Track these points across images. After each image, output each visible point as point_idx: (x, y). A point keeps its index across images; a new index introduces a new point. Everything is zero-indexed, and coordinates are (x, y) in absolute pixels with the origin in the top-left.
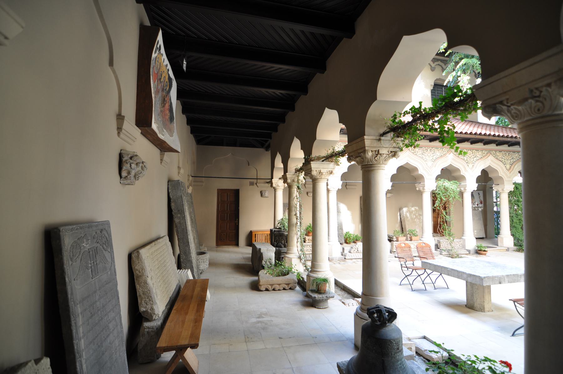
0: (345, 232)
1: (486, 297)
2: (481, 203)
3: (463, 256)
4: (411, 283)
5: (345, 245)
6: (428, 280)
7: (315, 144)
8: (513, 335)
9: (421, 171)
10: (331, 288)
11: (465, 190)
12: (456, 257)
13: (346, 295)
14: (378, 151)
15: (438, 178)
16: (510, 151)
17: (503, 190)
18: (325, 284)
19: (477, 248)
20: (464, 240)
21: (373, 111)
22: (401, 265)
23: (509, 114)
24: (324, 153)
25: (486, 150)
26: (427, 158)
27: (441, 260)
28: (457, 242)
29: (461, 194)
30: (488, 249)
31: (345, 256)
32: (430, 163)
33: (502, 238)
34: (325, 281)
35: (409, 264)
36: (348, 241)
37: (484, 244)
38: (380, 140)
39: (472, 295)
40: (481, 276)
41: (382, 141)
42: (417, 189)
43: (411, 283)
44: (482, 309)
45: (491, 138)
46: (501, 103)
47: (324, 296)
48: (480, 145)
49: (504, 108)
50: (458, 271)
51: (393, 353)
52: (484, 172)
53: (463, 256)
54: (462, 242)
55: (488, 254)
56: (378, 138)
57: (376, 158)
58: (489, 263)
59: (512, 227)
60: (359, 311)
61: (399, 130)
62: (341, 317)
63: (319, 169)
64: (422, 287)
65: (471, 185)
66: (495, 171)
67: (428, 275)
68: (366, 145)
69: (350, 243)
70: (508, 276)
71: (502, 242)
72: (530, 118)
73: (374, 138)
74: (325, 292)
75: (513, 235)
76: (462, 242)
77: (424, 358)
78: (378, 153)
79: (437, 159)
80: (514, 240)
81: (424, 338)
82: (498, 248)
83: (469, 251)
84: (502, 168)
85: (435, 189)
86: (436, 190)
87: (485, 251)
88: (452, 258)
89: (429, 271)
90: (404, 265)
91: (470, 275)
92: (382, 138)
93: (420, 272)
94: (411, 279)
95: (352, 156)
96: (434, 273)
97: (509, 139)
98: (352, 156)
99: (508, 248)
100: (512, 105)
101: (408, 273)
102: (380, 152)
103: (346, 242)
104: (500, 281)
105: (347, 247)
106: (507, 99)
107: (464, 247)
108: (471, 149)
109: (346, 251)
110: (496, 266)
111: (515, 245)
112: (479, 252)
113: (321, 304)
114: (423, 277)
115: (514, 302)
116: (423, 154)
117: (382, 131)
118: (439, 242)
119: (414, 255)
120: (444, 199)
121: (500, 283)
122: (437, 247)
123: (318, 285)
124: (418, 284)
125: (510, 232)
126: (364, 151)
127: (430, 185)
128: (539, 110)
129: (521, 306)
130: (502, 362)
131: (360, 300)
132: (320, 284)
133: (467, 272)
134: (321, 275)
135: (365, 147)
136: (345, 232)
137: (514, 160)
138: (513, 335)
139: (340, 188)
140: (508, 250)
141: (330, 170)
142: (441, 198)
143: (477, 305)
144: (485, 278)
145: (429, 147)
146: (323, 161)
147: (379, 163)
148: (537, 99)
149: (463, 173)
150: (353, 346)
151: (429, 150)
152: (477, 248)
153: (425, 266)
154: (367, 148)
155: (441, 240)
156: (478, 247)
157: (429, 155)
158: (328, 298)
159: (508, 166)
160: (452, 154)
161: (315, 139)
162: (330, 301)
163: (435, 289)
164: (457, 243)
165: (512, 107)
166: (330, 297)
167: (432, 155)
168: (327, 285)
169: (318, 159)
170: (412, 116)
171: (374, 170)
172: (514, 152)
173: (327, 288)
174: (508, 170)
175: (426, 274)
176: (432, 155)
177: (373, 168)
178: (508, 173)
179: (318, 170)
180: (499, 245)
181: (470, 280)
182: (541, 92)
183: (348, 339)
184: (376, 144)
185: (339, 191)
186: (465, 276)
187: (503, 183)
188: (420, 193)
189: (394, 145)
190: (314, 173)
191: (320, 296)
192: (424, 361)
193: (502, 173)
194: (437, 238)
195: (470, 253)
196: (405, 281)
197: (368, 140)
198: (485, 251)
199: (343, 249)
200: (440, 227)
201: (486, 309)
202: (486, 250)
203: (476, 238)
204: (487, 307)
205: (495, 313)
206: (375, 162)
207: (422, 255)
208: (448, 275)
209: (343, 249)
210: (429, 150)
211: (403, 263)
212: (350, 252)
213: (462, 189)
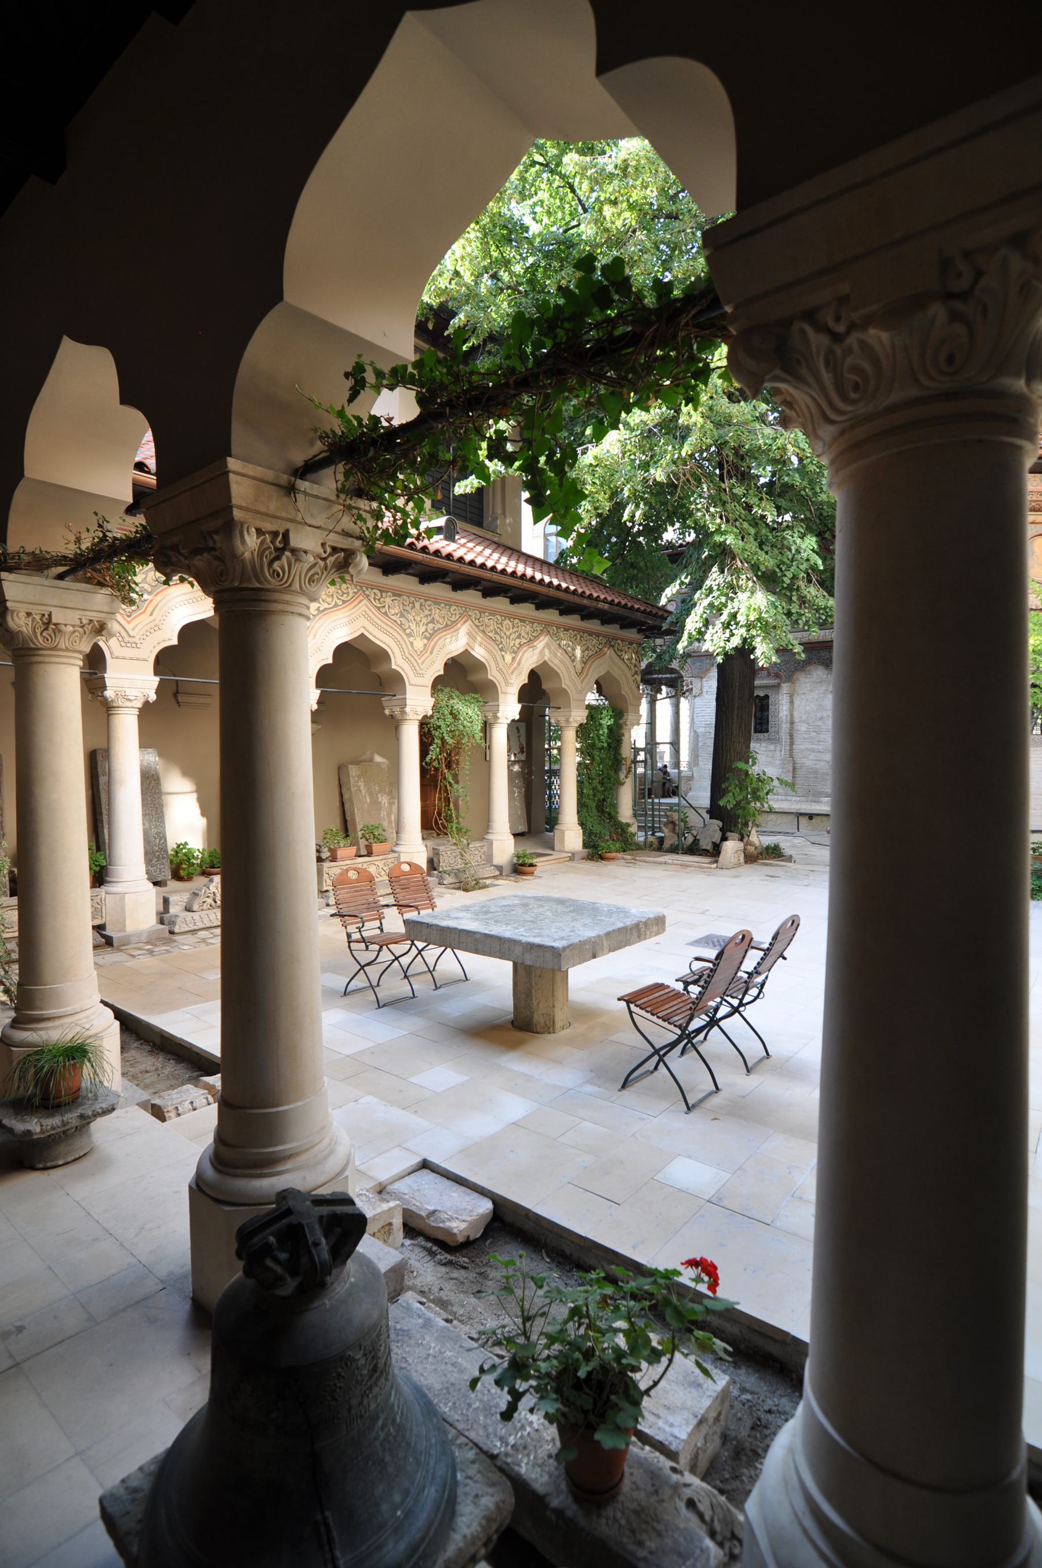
0: (171, 845)
1: (559, 994)
2: (522, 752)
3: (488, 882)
4: (375, 983)
5: (173, 884)
6: (419, 966)
7: (20, 496)
8: (623, 1087)
9: (398, 663)
10: (110, 1061)
11: (496, 717)
12: (474, 889)
13: (170, 1067)
14: (286, 535)
15: (438, 684)
16: (584, 632)
17: (567, 721)
18: (77, 1069)
19: (515, 860)
20: (490, 843)
21: (266, 351)
22: (349, 936)
23: (826, 377)
24: (62, 542)
25: (539, 622)
26: (413, 627)
27: (450, 907)
28: (477, 849)
29: (486, 727)
30: (538, 860)
31: (172, 923)
32: (419, 643)
33: (563, 832)
34: (77, 1053)
35: (371, 929)
36: (182, 873)
37: (529, 847)
38: (290, 490)
39: (529, 995)
40: (556, 944)
41: (300, 497)
42: (387, 712)
43: (375, 983)
44: (549, 1028)
45: (552, 592)
46: (810, 315)
47: (71, 1117)
48: (526, 609)
49: (817, 340)
50: (499, 939)
51: (354, 1402)
52: (533, 675)
53: (488, 882)
54: (485, 849)
55: (538, 871)
56: (284, 479)
57: (276, 565)
58: (561, 902)
59: (581, 805)
60: (210, 1172)
61: (368, 458)
62: (146, 1165)
63: (45, 610)
64: (403, 988)
65: (510, 709)
66: (555, 675)
67: (420, 952)
68: (235, 501)
69: (189, 878)
70: (608, 934)
71: (562, 841)
72: (913, 392)
73: (270, 475)
74: (75, 1098)
75: (582, 824)
76: (485, 849)
77: (428, 1238)
78: (282, 545)
79: (435, 631)
80: (584, 834)
81: (425, 1165)
82: (556, 855)
83: (500, 868)
84: (567, 668)
85: (430, 713)
86: (432, 716)
87: (531, 865)
88: (466, 890)
89: (420, 945)
90: (356, 936)
91: (531, 947)
92: (303, 485)
93: (399, 949)
94: (373, 972)
95: (175, 548)
96: (431, 946)
97: (585, 602)
98: (175, 548)
99: (573, 854)
100: (852, 327)
101: (365, 957)
102: (295, 541)
103: (177, 876)
104: (590, 950)
105: (179, 894)
106: (843, 300)
107: (489, 858)
108: (511, 617)
109: (173, 910)
110: (577, 908)
111: (585, 845)
112: (520, 868)
113: (62, 1148)
114: (405, 961)
115: (628, 1002)
116: (402, 616)
117: (299, 457)
118: (436, 852)
119: (383, 901)
120: (450, 741)
121: (594, 957)
122: (432, 864)
123: (44, 1081)
124: (394, 986)
125: (576, 817)
126: (229, 527)
127: (418, 702)
128: (951, 359)
129: (643, 1013)
130: (692, 1263)
131: (215, 1080)
132: (52, 1072)
133: (524, 939)
134: (54, 1034)
135: (229, 508)
136: (171, 845)
137: (591, 653)
138: (623, 1087)
139: (153, 697)
140: (572, 857)
141: (95, 616)
142: (442, 739)
143: (538, 1018)
144: (564, 949)
145: (418, 596)
146: (61, 577)
147: (288, 589)
148: (958, 305)
149: (493, 674)
150: (186, 1307)
151: (417, 605)
152: (515, 860)
153: (415, 931)
154: (237, 514)
155: (441, 848)
156: (519, 857)
157: (418, 618)
158: (86, 1120)
159: (579, 666)
160: (469, 622)
161: (21, 475)
162: (98, 1126)
163: (436, 988)
164: (475, 851)
165: (852, 340)
166: (96, 1115)
167: (424, 620)
168: (87, 1070)
169: (38, 564)
170: (421, 400)
171: (268, 613)
172: (590, 634)
173: (85, 1084)
174: (579, 674)
175: (414, 951)
176: (424, 620)
177: (263, 606)
179: (36, 610)
180: (556, 848)
181: (529, 960)
182: (979, 274)
183: (167, 1284)
184: (274, 503)
185: (146, 711)
186: (518, 950)
187: (569, 706)
188: (394, 724)
189: (347, 523)
190: (19, 622)
191: (55, 1121)
192: (431, 1253)
193: (568, 682)
194: (429, 843)
195: (501, 874)
196: (360, 982)
197: (245, 480)
198: (531, 865)
199: (166, 902)
200: (439, 814)
201: (559, 1024)
202: (535, 861)
203: (515, 835)
204: (560, 1016)
205: (578, 1028)
206: (274, 582)
207: (405, 898)
208: (477, 951)
209: (166, 902)
210: (417, 605)
211: (352, 929)
212: (188, 909)
213: (490, 716)
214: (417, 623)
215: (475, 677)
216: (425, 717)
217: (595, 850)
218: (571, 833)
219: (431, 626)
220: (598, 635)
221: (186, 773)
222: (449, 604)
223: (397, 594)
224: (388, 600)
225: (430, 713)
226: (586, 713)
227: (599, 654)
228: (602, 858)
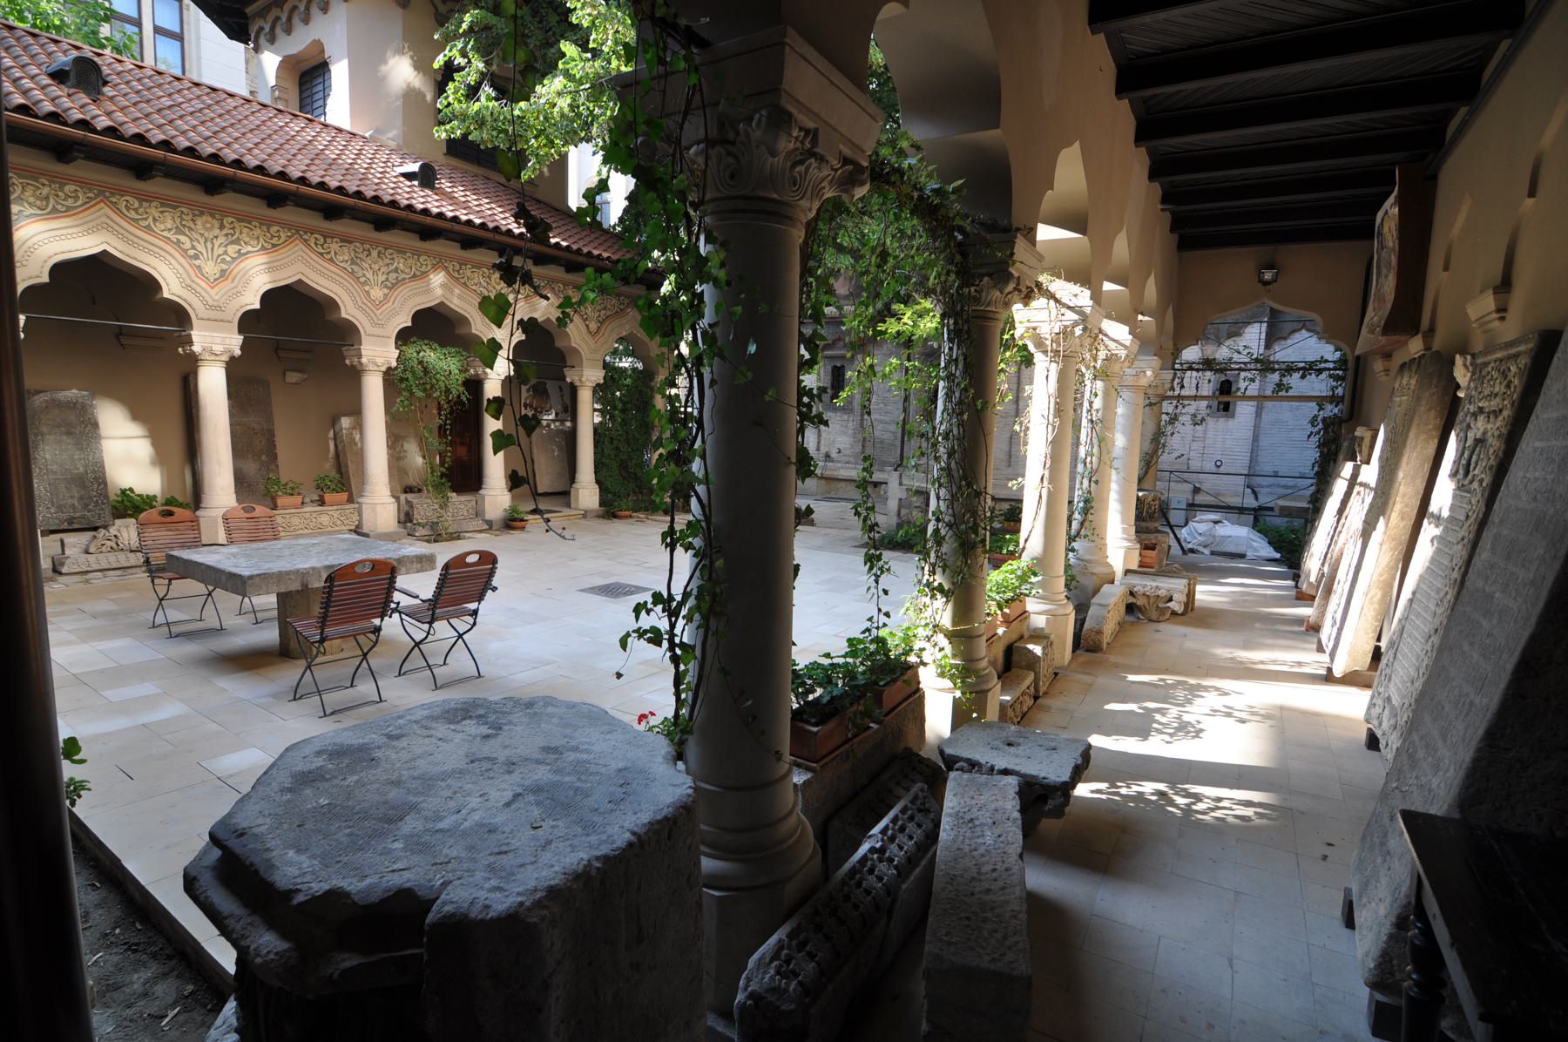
2: (566, 411)
9: (349, 310)
15: (403, 337)
32: (377, 293)
71: (577, 499)
79: (399, 282)
85: (394, 364)
116: (353, 262)
127: (378, 352)
140: (585, 515)
151: (375, 253)
159: (593, 326)
174: (593, 335)
178: (588, 338)
188: (355, 375)
210: (375, 253)
214: (375, 272)
215: (461, 331)
216: (389, 369)
217: (610, 509)
218: (587, 493)
219: (394, 275)
220: (619, 295)
221: (136, 415)
222: (417, 253)
223: (346, 240)
224: (335, 246)
225: (394, 364)
226: (603, 373)
227: (620, 313)
228: (615, 516)
